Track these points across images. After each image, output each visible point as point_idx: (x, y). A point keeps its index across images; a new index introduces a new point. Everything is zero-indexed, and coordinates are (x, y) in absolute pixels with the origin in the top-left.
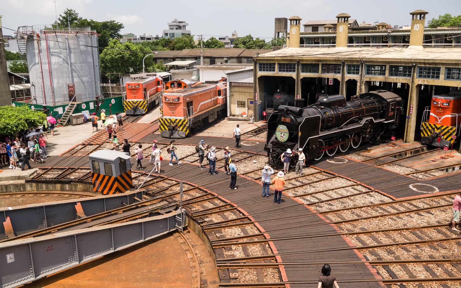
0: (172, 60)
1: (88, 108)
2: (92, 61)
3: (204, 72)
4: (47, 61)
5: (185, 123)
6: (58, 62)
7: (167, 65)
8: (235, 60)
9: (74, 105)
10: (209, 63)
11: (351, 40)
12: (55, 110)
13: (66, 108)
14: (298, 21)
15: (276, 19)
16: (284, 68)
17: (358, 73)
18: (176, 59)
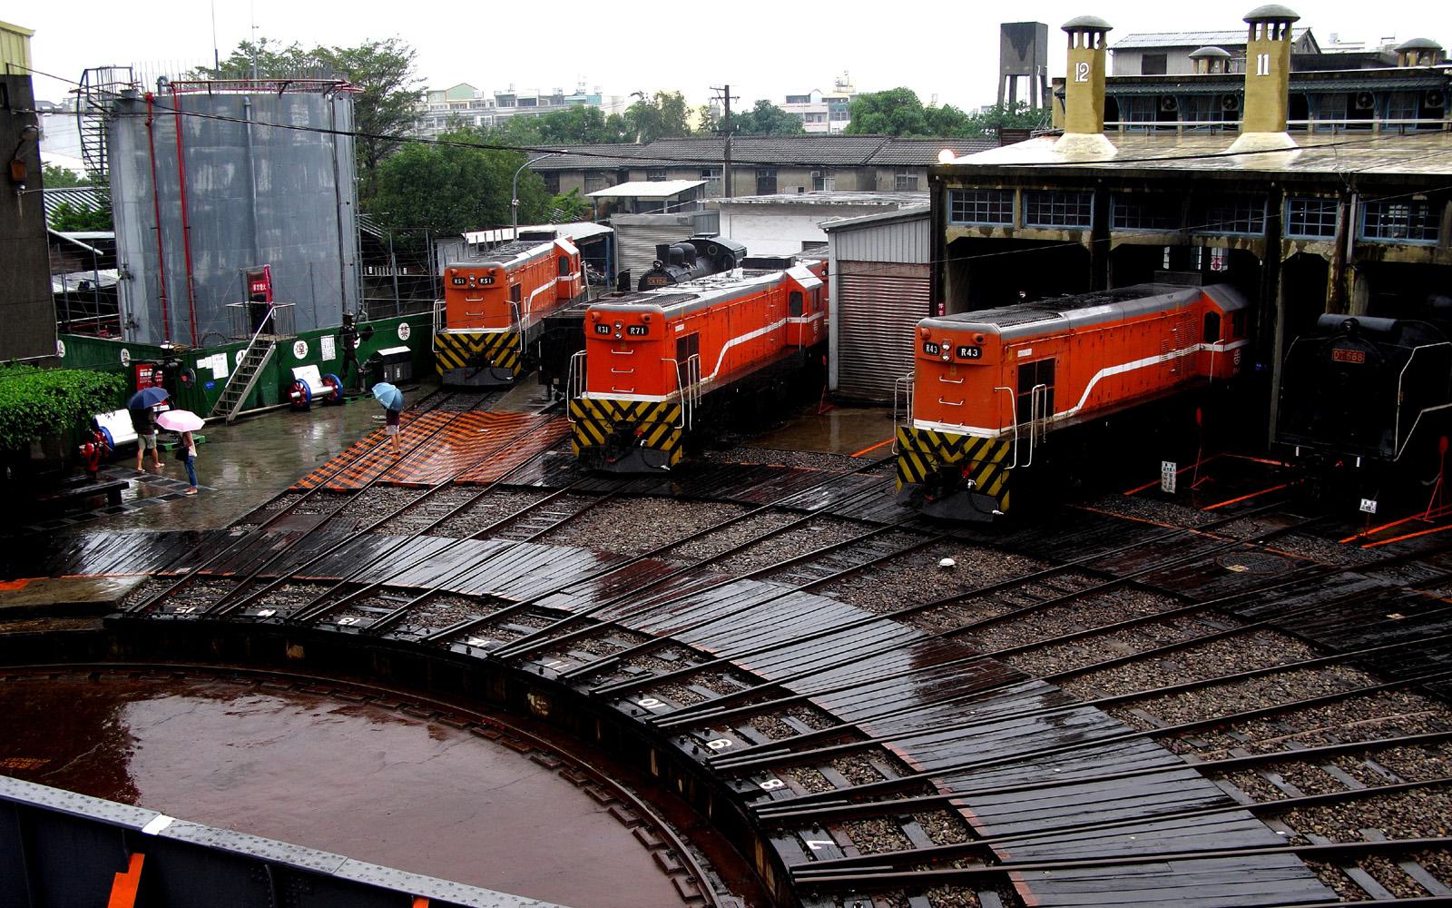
0: (614, 178)
1: (314, 357)
2: (332, 185)
3: (734, 223)
4: (177, 188)
5: (671, 418)
6: (213, 190)
7: (596, 198)
8: (851, 177)
9: (267, 344)
10: (754, 189)
11: (1297, 108)
12: (201, 364)
13: (240, 356)
14: (1097, 36)
15: (1004, 26)
16: (1047, 209)
17: (1329, 231)
18: (630, 175)
